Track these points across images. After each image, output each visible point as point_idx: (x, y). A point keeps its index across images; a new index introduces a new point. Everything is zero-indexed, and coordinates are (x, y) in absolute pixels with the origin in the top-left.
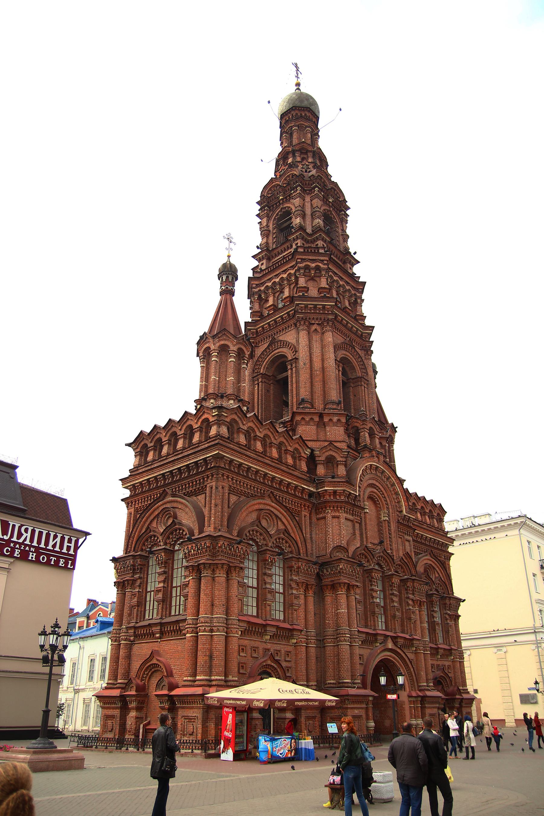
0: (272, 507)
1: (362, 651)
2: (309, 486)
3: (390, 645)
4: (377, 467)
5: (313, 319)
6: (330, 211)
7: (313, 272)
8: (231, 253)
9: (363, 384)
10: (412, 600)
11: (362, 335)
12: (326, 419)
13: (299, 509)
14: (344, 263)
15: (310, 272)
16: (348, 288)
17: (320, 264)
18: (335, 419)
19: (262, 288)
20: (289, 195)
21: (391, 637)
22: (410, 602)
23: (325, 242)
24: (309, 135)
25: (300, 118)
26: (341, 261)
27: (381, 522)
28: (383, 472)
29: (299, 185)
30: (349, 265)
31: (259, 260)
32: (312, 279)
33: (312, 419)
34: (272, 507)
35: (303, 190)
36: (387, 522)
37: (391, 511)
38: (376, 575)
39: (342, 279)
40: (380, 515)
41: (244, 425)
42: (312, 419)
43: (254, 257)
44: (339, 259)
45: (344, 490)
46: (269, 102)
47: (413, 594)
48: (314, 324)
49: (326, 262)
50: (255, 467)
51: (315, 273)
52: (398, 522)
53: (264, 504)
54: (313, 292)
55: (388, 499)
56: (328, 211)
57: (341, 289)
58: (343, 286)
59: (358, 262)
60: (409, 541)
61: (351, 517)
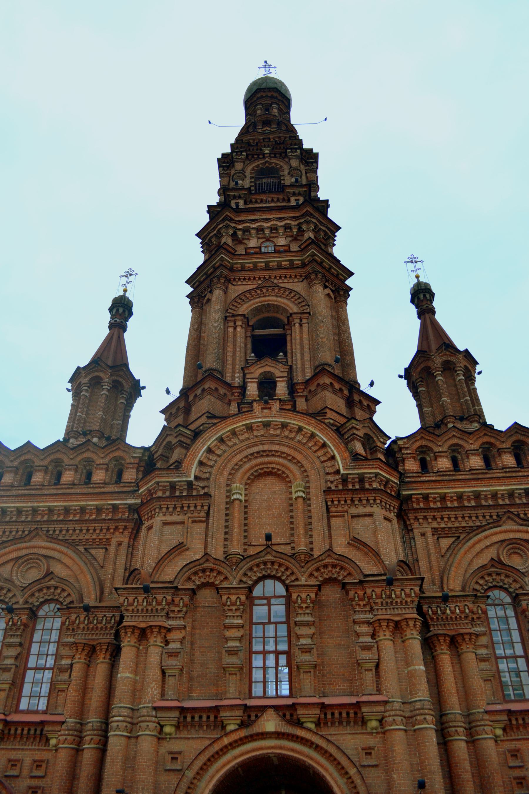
0: (43, 548)
1: (176, 746)
2: (126, 499)
3: (270, 723)
4: (266, 425)
5: (205, 290)
6: (267, 162)
8: (129, 287)
9: (297, 321)
10: (369, 623)
13: (108, 536)
14: (289, 201)
16: (282, 224)
18: (199, 391)
21: (276, 708)
22: (364, 629)
23: (240, 197)
26: (284, 200)
27: (291, 505)
28: (284, 426)
34: (43, 548)
36: (300, 500)
37: (313, 478)
38: (233, 598)
39: (267, 220)
40: (291, 493)
41: (12, 461)
44: (278, 200)
45: (158, 483)
47: (372, 610)
50: (13, 505)
52: (328, 491)
53: (27, 548)
55: (305, 463)
57: (267, 232)
60: (370, 515)
61: (181, 518)
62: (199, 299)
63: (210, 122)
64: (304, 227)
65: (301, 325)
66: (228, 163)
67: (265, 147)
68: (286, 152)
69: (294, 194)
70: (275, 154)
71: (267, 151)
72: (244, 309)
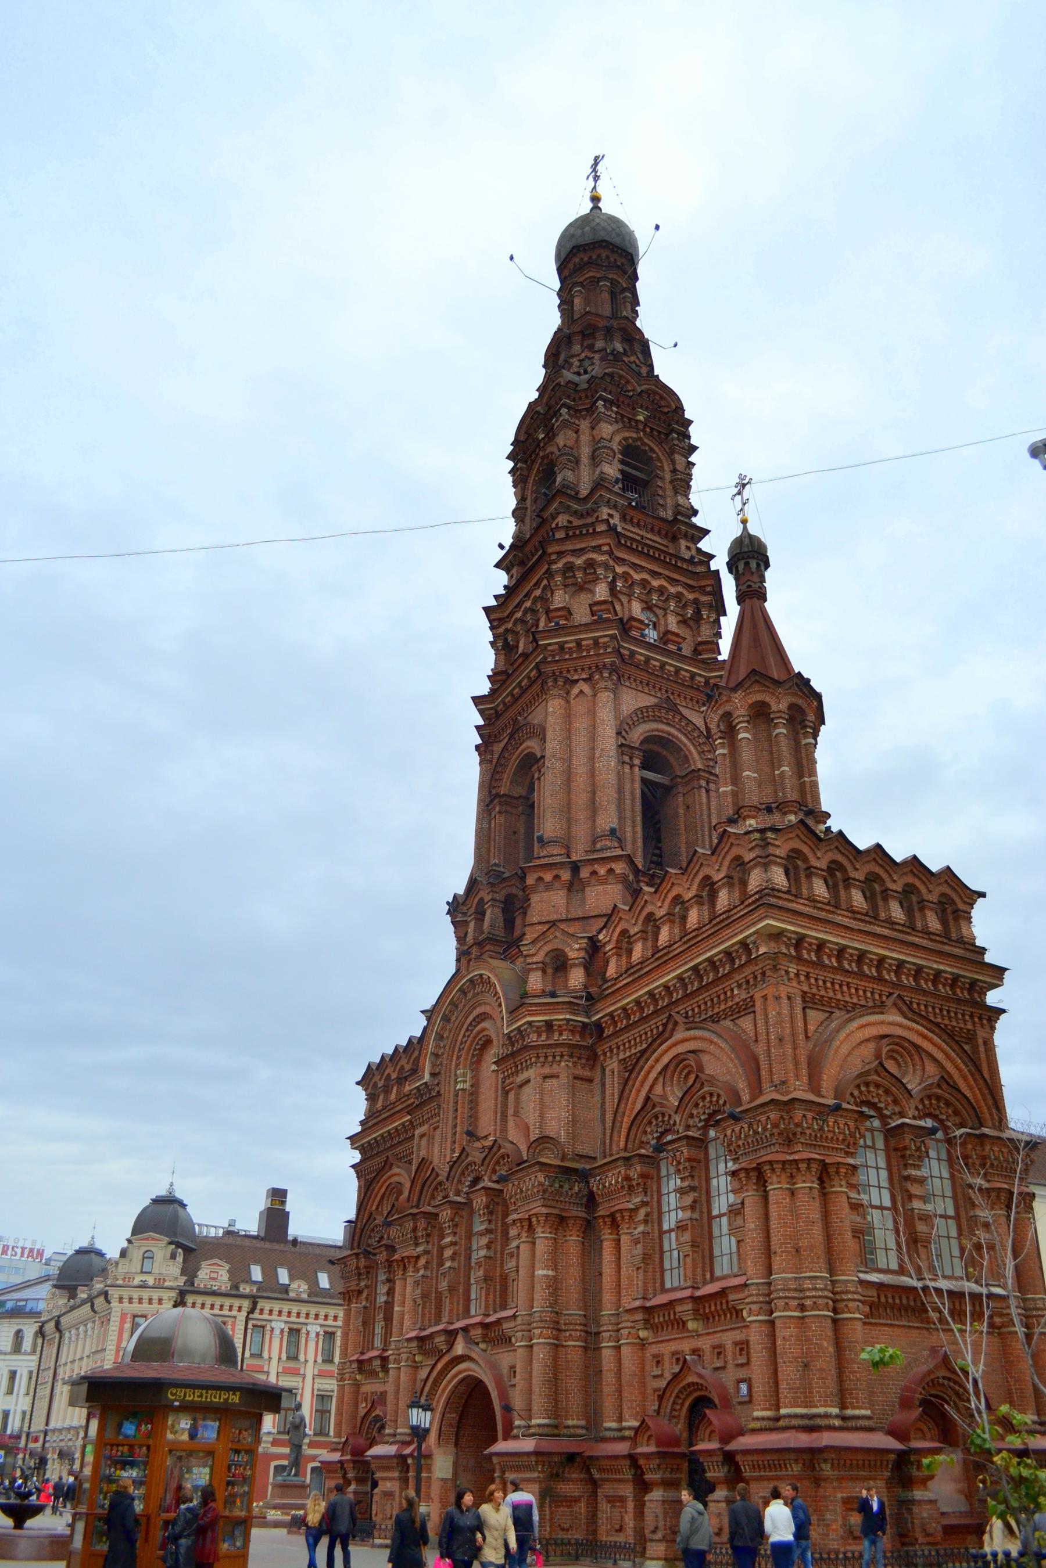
6: (640, 439)
7: (579, 575)
9: (703, 783)
11: (707, 683)
12: (584, 873)
14: (674, 539)
15: (574, 576)
17: (595, 556)
19: (510, 625)
20: (552, 428)
23: (615, 507)
24: (606, 296)
25: (597, 263)
29: (565, 405)
30: (683, 543)
31: (508, 570)
32: (581, 588)
33: (557, 877)
35: (575, 412)
39: (655, 574)
42: (557, 877)
43: (497, 566)
46: (512, 258)
48: (577, 681)
49: (605, 548)
51: (585, 574)
54: (581, 615)
56: (635, 440)
58: (661, 590)
59: (706, 532)
62: (565, 683)
63: (512, 258)
64: (705, 613)
65: (708, 791)
66: (574, 400)
67: (641, 407)
68: (667, 435)
69: (686, 535)
70: (652, 429)
71: (641, 418)
72: (636, 735)
